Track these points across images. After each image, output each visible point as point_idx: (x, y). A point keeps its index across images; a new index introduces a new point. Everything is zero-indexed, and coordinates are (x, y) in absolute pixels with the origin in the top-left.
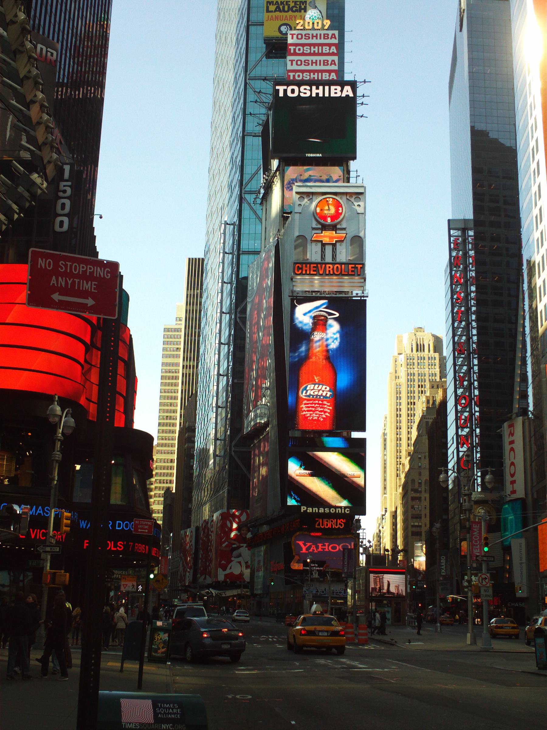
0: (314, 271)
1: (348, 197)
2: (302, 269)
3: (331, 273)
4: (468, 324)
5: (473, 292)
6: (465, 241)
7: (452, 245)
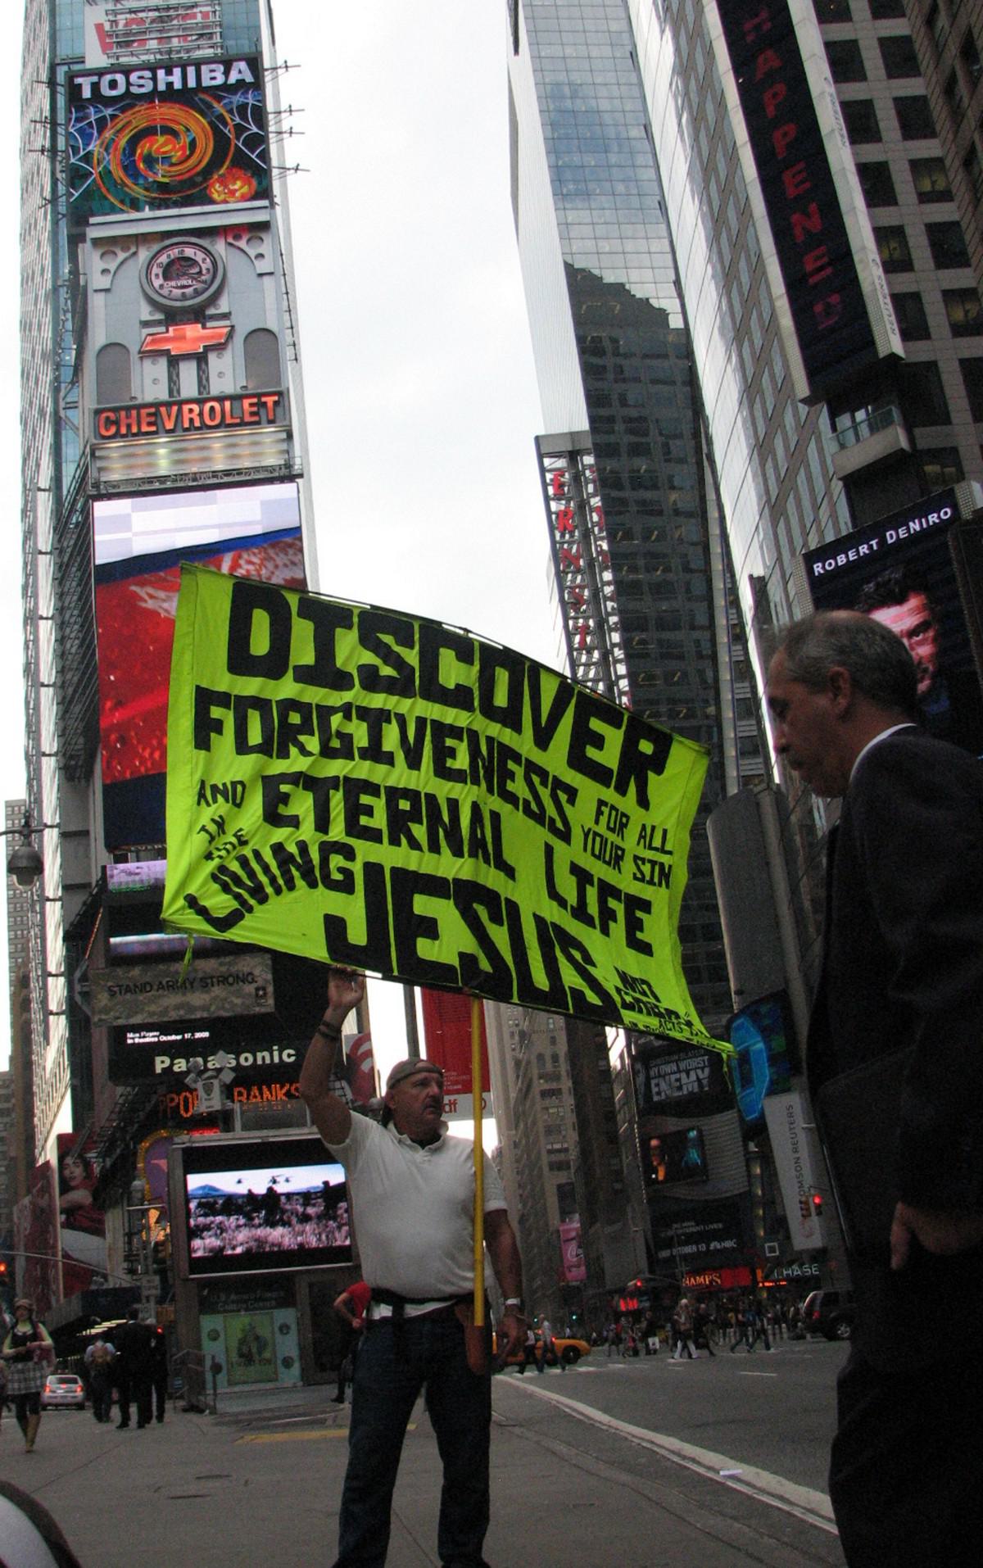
0: (150, 424)
1: (230, 240)
2: (117, 423)
3: (197, 424)
4: (606, 654)
5: (609, 583)
6: (577, 478)
7: (551, 490)
